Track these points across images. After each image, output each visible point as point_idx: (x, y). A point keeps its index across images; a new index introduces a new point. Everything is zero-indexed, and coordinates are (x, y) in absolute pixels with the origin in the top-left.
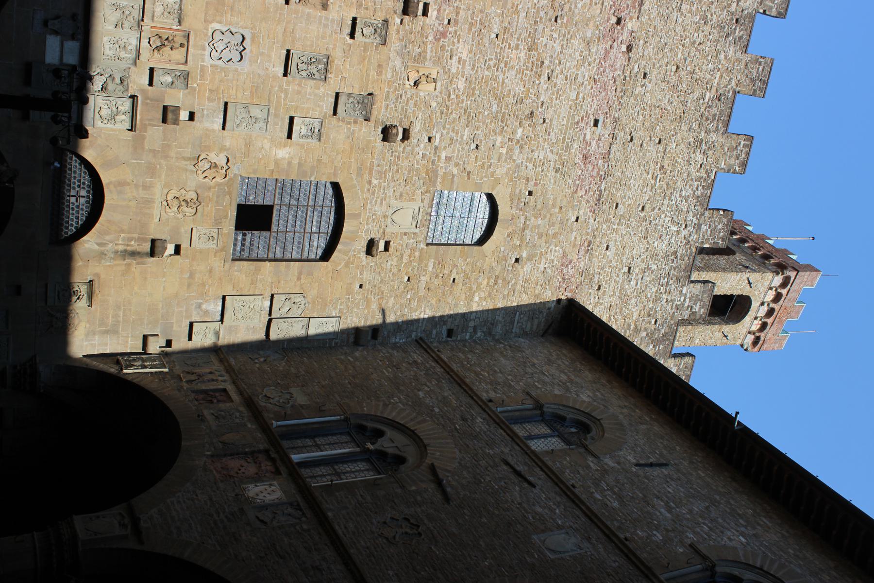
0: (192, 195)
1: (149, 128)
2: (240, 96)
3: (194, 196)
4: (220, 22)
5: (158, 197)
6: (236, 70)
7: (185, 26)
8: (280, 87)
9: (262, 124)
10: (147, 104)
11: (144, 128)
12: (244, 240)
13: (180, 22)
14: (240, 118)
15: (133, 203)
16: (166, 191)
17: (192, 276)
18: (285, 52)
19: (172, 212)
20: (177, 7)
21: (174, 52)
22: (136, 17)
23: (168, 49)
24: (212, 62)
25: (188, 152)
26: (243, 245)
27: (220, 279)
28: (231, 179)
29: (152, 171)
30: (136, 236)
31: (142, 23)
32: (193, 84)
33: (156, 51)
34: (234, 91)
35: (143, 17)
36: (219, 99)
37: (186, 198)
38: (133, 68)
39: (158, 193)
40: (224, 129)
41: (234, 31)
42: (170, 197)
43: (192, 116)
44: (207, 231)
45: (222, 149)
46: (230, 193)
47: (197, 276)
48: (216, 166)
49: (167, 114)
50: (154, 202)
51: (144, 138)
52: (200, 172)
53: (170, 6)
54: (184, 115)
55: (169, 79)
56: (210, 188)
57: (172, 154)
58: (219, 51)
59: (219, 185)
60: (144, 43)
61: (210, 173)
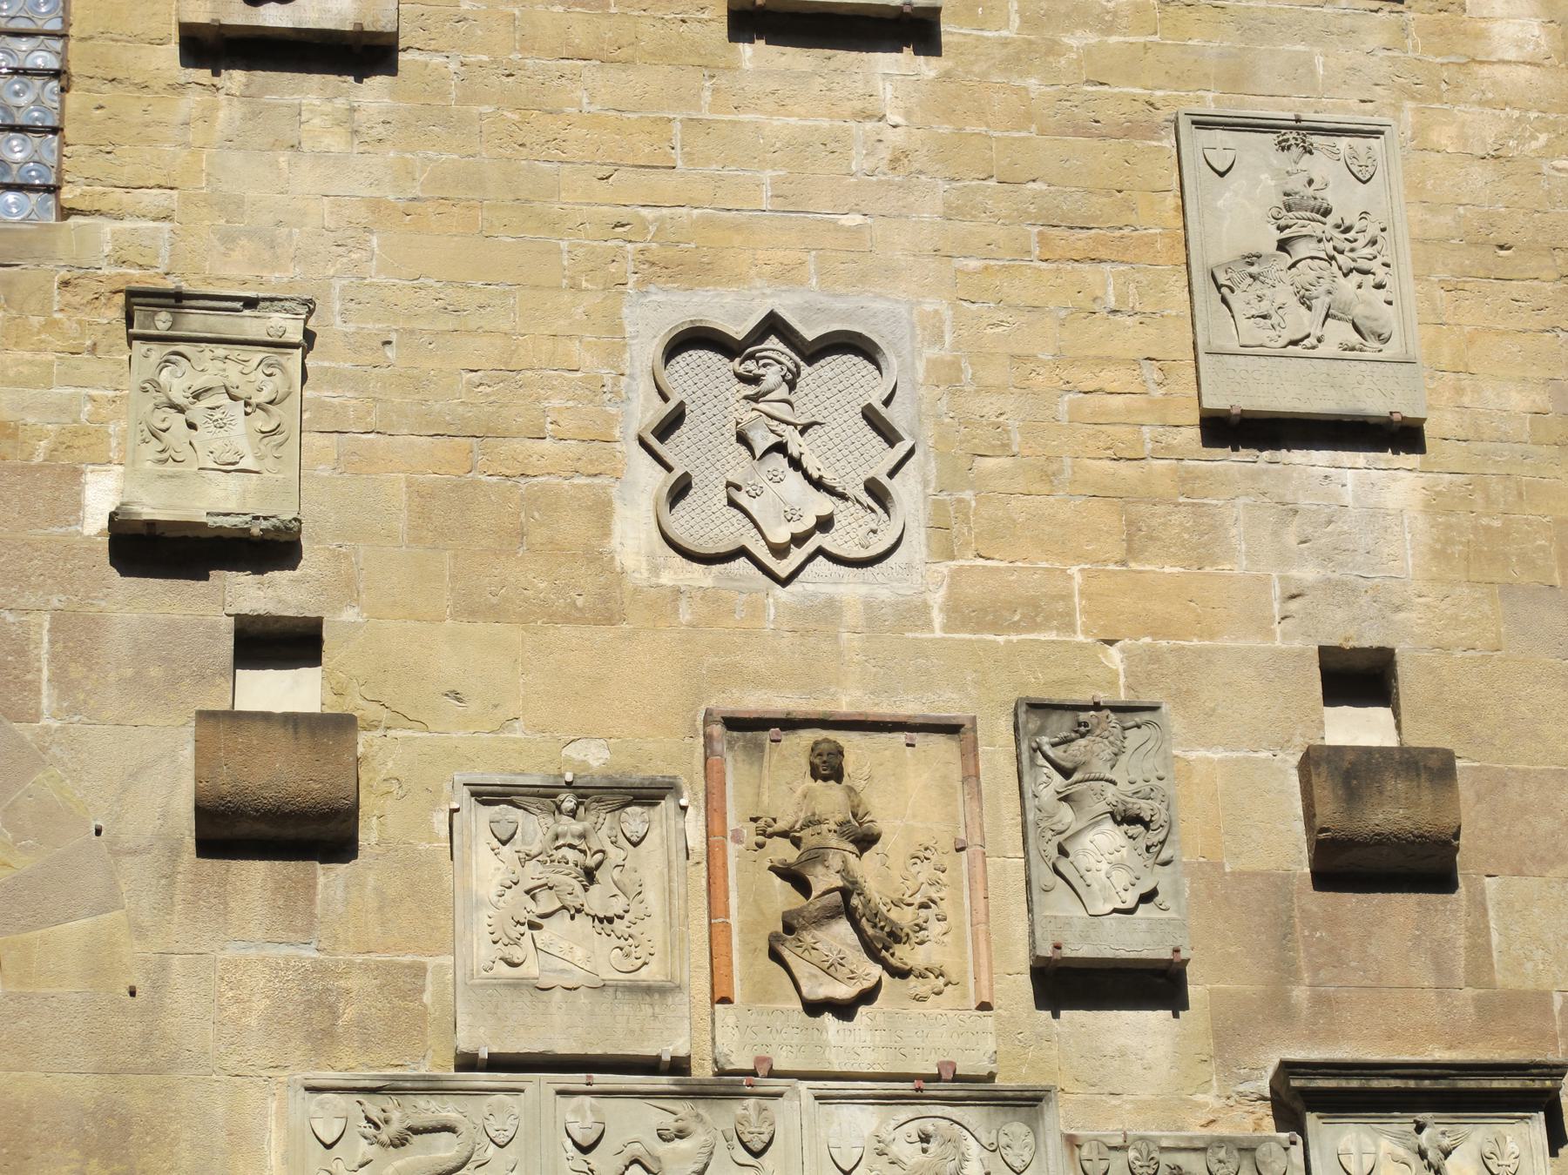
1: (1503, 978)
2: (1131, 337)
4: (602, 512)
6: (948, 376)
7: (669, 751)
8: (1017, 58)
9: (1324, 166)
10: (1322, 1002)
11: (1501, 1007)
13: (648, 795)
14: (1301, 321)
18: (753, 53)
20: (534, 827)
21: (882, 818)
22: (653, 1116)
23: (867, 868)
24: (915, 548)
31: (703, 1071)
32: (1112, 674)
33: (903, 955)
34: (1110, 377)
35: (650, 1066)
36: (1186, 481)
38: (1058, 1119)
40: (1401, 436)
41: (647, 411)
43: (1358, 677)
49: (1381, 852)
53: (533, 874)
54: (1360, 728)
55: (1103, 850)
58: (824, 504)
60: (849, 1045)
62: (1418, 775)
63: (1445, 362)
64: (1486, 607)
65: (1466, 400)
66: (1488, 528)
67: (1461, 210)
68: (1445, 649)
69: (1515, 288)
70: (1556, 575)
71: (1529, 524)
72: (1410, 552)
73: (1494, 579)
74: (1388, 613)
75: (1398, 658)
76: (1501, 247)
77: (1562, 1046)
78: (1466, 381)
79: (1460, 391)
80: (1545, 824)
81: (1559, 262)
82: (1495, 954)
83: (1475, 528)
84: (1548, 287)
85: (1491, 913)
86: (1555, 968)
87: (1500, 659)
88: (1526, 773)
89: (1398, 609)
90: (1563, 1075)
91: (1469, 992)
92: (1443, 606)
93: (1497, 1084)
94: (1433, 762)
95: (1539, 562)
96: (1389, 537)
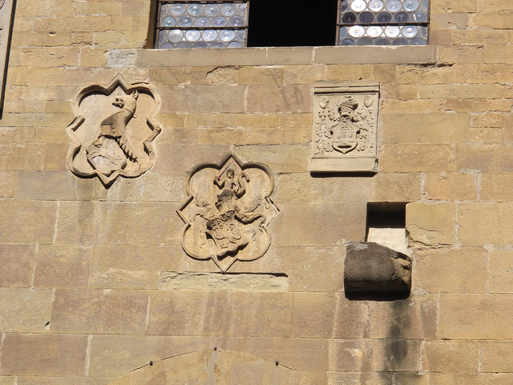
0: (203, 186)
5: (209, 283)
15: (225, 360)
16: (188, 264)
17: (479, 162)
19: (256, 239)
25: (65, 207)
27: (490, 72)
28: (154, 75)
29: (124, 307)
30: (333, 345)
37: (212, 201)
45: (57, 109)
47: (477, 144)
48: (110, 122)
50: (222, 296)
52: (131, 169)
56: (181, 134)
57: (68, 253)
59: (170, 109)
61: (134, 135)
63: (17, 82)
64: (11, 180)
65: (22, 97)
66: (19, 149)
67: (38, 19)
69: (52, 50)
70: (42, 166)
71: (36, 146)
73: (17, 169)
76: (51, 33)
78: (24, 88)
79: (20, 93)
80: (15, 266)
81: (72, 37)
83: (14, 148)
84: (66, 48)
87: (13, 201)
88: (12, 246)
95: (37, 161)
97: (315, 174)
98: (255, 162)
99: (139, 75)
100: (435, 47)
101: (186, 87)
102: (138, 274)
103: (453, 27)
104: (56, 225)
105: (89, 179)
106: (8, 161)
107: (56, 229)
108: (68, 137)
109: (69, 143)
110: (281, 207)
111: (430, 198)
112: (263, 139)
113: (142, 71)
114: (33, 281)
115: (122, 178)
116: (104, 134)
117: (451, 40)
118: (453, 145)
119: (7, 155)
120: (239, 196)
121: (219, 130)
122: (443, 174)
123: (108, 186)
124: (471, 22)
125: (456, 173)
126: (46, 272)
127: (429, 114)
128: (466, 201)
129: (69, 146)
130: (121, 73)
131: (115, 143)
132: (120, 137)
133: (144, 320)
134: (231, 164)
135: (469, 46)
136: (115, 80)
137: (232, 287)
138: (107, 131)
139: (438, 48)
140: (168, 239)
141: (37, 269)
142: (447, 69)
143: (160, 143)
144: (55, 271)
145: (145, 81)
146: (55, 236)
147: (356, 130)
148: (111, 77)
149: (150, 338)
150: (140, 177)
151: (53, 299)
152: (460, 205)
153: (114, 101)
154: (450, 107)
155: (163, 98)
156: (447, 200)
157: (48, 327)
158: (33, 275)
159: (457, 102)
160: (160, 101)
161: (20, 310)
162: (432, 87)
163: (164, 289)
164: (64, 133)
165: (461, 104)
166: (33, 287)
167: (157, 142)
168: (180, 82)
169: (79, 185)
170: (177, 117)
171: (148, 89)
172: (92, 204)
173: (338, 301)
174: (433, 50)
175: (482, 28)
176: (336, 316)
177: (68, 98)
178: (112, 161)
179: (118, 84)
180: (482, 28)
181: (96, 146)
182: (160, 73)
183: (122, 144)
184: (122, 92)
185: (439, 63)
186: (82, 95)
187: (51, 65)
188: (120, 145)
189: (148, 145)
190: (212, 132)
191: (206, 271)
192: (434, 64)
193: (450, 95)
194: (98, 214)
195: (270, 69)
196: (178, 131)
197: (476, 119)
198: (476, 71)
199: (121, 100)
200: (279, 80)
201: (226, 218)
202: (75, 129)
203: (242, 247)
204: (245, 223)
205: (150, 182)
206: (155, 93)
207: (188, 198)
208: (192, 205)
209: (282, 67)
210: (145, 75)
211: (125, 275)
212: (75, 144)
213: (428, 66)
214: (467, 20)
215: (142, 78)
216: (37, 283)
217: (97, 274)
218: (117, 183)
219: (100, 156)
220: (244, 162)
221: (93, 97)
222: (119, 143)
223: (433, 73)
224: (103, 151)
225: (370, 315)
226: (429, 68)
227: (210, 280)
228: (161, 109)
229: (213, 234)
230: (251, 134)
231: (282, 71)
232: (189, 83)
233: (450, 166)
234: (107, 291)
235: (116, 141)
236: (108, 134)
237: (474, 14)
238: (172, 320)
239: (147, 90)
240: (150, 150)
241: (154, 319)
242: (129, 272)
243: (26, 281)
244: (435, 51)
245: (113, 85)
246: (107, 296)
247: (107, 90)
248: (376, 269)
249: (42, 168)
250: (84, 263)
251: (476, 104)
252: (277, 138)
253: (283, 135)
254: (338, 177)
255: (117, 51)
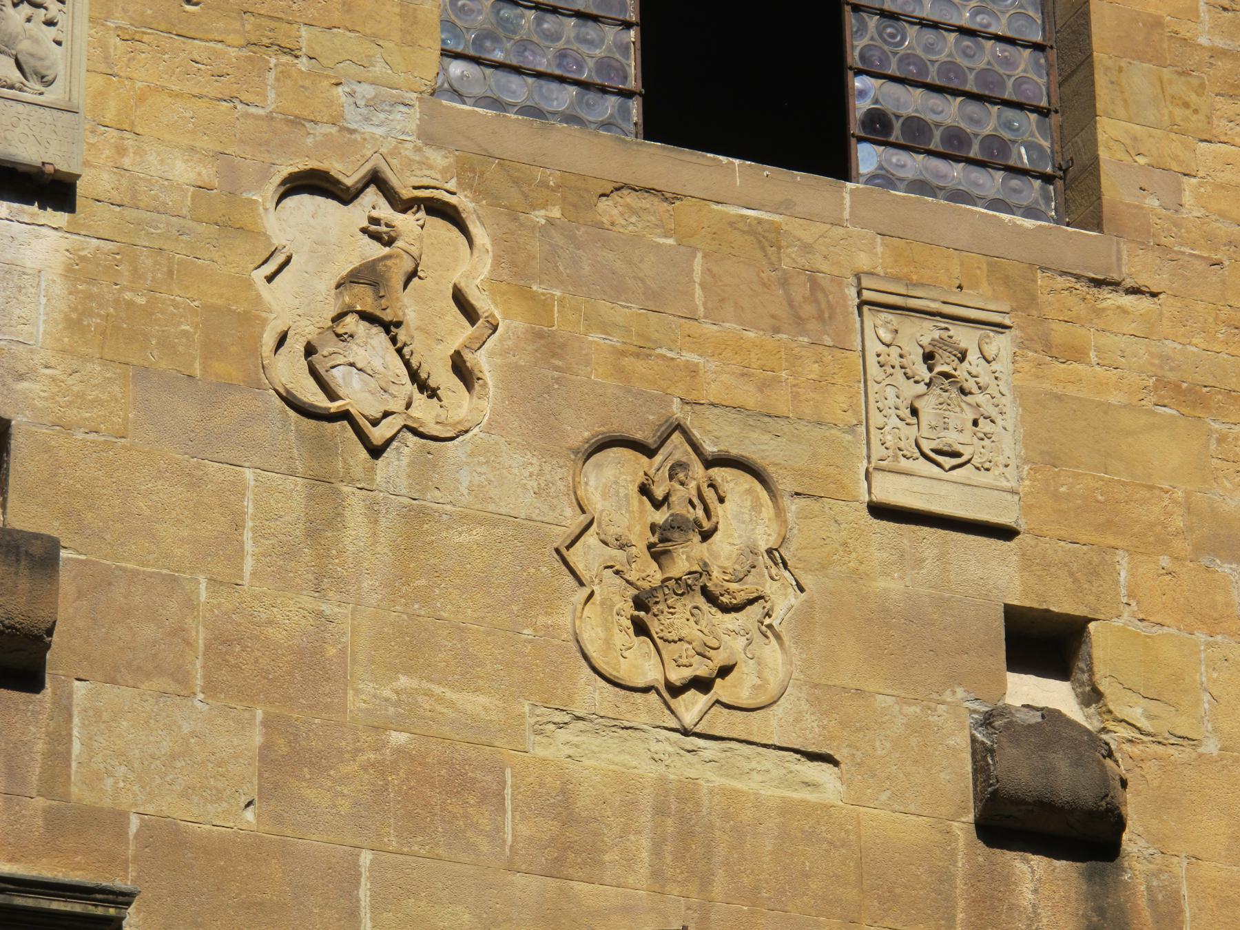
3: (614, 476)
11: (70, 822)
12: (915, 137)
16: (596, 696)
25: (268, 488)
26: (954, 148)
28: (467, 171)
29: (441, 790)
37: (640, 538)
39: (619, 758)
42: (642, 665)
44: (891, 393)
46: (581, 194)
48: (367, 276)
50: (688, 792)
51: (166, 840)
52: (424, 412)
56: (548, 345)
57: (289, 615)
59: (515, 271)
62: (18, 561)
63: (110, 116)
65: (127, 162)
66: (130, 304)
68: (66, 428)
70: (197, 365)
71: (176, 306)
72: (43, 318)
73: (130, 360)
74: (9, 380)
75: (13, 430)
77: (132, 873)
78: (130, 141)
79: (121, 150)
80: (148, 631)
81: (248, 27)
82: (74, 765)
84: (233, 52)
85: (76, 720)
86: (136, 788)
88: (135, 573)
89: (21, 377)
90: (129, 904)
91: (40, 802)
92: (70, 381)
93: (57, 905)
94: (37, 549)
95: (181, 349)
96: (22, 298)
97: (880, 511)
98: (734, 452)
99: (430, 167)
100: (1118, 244)
101: (551, 222)
102: (477, 703)
103: (1152, 202)
104: (248, 536)
105: (326, 424)
106: (103, 334)
107: (249, 546)
108: (259, 296)
109: (264, 315)
110: (806, 581)
111: (1141, 616)
112: (749, 396)
113: (438, 158)
114: (199, 682)
115: (409, 435)
116: (359, 308)
117: (1149, 231)
118: (1179, 495)
119: (99, 315)
120: (706, 536)
121: (642, 352)
122: (1165, 561)
123: (376, 452)
124: (1187, 198)
125: (1191, 564)
126: (233, 661)
127: (1120, 407)
128: (1219, 638)
129: (264, 322)
130: (384, 150)
131: (383, 337)
132: (398, 324)
133: (499, 829)
134: (677, 447)
135: (1191, 255)
136: (368, 167)
137: (706, 769)
138: (364, 299)
139: (1124, 247)
140: (542, 620)
141: (208, 647)
142: (1144, 303)
143: (498, 360)
144: (256, 662)
145: (448, 186)
146: (249, 565)
147: (970, 415)
148: (358, 157)
149: (519, 879)
150: (456, 442)
151: (258, 740)
152: (1209, 645)
153: (365, 224)
154: (1163, 397)
155: (494, 241)
156: (1179, 629)
157: (249, 815)
158: (199, 663)
159: (1177, 387)
160: (489, 247)
161: (174, 757)
162: (1122, 342)
163: (541, 752)
164: (249, 284)
165: (1188, 396)
166: (201, 696)
167: (491, 355)
168: (534, 207)
169: (301, 436)
170: (533, 297)
171: (454, 208)
172: (337, 492)
173: (961, 844)
174: (1114, 248)
175: (1214, 218)
176: (959, 882)
177: (250, 191)
178: (384, 385)
179: (376, 179)
180: (1214, 218)
181: (338, 335)
182: (482, 173)
183: (405, 345)
184: (382, 202)
185: (1129, 283)
186: (282, 189)
187: (196, 91)
188: (399, 345)
189: (467, 356)
190: (623, 354)
191: (641, 719)
192: (1117, 284)
193: (1161, 367)
194: (356, 526)
195: (747, 217)
196: (539, 335)
197: (1221, 440)
198: (1211, 320)
199: (387, 225)
200: (771, 251)
201: (682, 587)
202: (270, 279)
203: (724, 671)
204: (726, 609)
205: (482, 459)
206: (474, 222)
207: (583, 519)
208: (590, 539)
209: (776, 218)
210: (445, 170)
211: (440, 700)
212: (279, 322)
213: (1104, 287)
214: (1179, 191)
215: (438, 177)
216: (211, 688)
217: (368, 687)
218: (397, 448)
219: (352, 365)
220: (710, 448)
221: (305, 199)
222: (394, 340)
223: (1118, 307)
224: (358, 353)
225: (1035, 891)
226: (1105, 292)
227: (655, 747)
228: (493, 270)
229: (654, 627)
230: (718, 381)
231: (777, 229)
232: (556, 212)
233: (1178, 544)
234: (398, 738)
235: (388, 332)
236: (369, 309)
237: (1193, 180)
238: (571, 839)
239: (450, 211)
240: (471, 372)
241: (525, 830)
242: (450, 694)
243: (182, 678)
244: (1119, 251)
245: (362, 178)
246: (399, 750)
247: (348, 188)
248: (1066, 780)
249: (197, 370)
250: (332, 651)
251: (1219, 401)
252: (781, 401)
253: (795, 396)
254: (931, 526)
255: (367, 90)
